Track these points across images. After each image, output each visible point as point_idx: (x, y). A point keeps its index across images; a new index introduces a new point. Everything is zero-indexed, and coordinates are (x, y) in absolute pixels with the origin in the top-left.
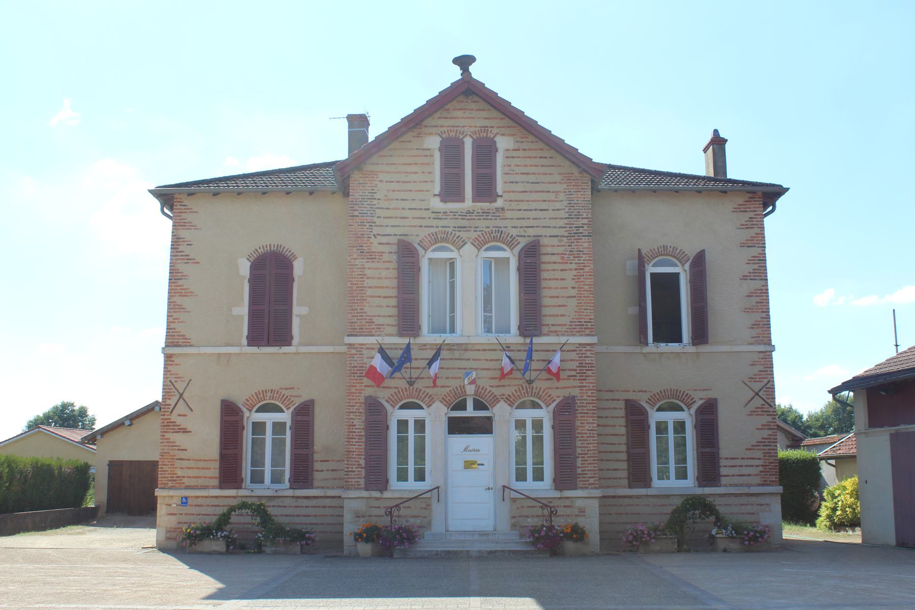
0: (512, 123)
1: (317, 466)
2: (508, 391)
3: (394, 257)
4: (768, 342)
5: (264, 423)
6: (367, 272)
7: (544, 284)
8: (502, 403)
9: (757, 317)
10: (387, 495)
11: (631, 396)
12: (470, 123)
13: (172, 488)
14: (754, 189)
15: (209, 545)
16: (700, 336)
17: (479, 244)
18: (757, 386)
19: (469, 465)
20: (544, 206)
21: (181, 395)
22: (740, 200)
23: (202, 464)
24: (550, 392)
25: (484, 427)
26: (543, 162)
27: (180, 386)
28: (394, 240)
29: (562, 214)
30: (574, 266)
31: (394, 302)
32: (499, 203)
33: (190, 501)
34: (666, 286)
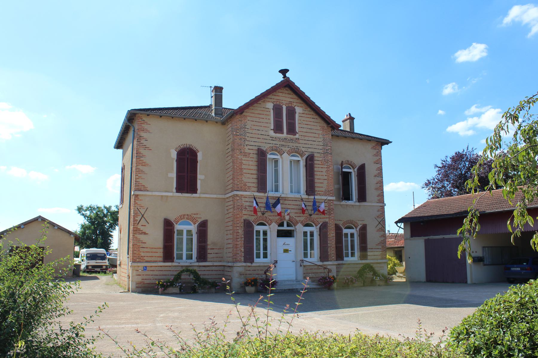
0: (301, 102)
1: (209, 251)
2: (302, 219)
3: (255, 156)
4: (383, 202)
5: (182, 231)
6: (243, 161)
7: (316, 173)
8: (300, 223)
9: (379, 192)
10: (254, 264)
11: (338, 222)
12: (287, 99)
13: (139, 262)
14: (379, 140)
15: (171, 290)
16: (362, 197)
17: (289, 153)
18: (379, 220)
19: (286, 251)
20: (314, 139)
21: (143, 216)
22: (374, 145)
23: (154, 250)
24: (318, 220)
25: (288, 234)
26: (313, 120)
27: (142, 211)
28: (256, 148)
29: (321, 144)
30: (326, 166)
31: (255, 176)
32: (297, 136)
33: (148, 269)
34: (346, 177)
